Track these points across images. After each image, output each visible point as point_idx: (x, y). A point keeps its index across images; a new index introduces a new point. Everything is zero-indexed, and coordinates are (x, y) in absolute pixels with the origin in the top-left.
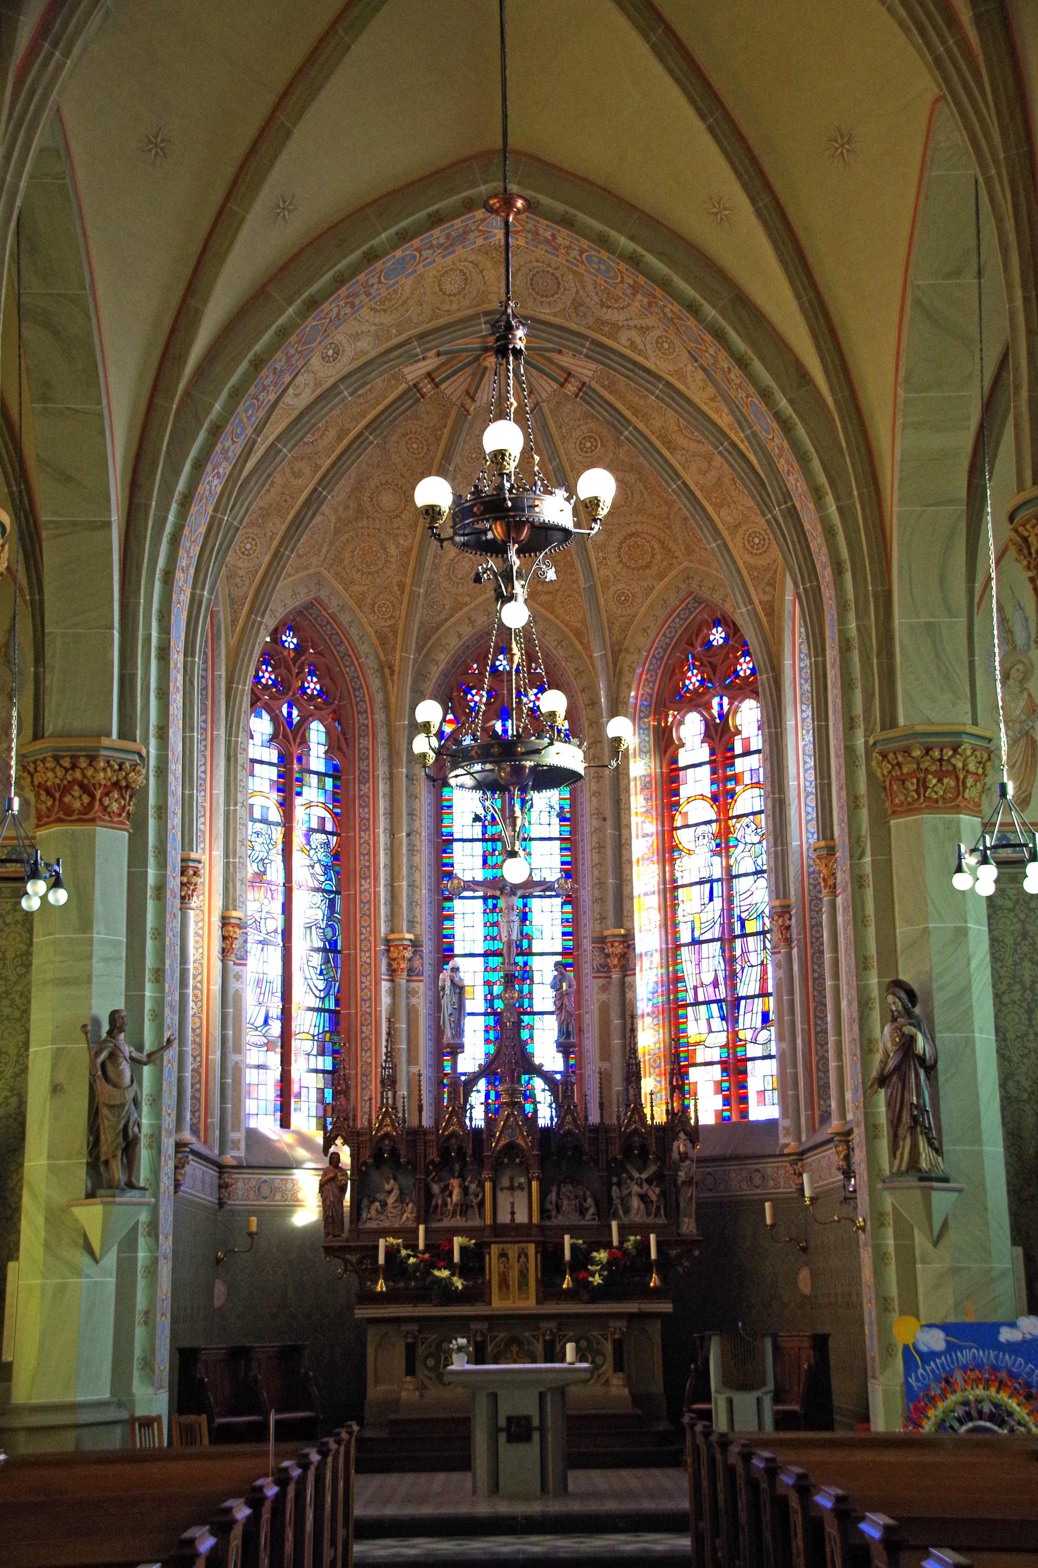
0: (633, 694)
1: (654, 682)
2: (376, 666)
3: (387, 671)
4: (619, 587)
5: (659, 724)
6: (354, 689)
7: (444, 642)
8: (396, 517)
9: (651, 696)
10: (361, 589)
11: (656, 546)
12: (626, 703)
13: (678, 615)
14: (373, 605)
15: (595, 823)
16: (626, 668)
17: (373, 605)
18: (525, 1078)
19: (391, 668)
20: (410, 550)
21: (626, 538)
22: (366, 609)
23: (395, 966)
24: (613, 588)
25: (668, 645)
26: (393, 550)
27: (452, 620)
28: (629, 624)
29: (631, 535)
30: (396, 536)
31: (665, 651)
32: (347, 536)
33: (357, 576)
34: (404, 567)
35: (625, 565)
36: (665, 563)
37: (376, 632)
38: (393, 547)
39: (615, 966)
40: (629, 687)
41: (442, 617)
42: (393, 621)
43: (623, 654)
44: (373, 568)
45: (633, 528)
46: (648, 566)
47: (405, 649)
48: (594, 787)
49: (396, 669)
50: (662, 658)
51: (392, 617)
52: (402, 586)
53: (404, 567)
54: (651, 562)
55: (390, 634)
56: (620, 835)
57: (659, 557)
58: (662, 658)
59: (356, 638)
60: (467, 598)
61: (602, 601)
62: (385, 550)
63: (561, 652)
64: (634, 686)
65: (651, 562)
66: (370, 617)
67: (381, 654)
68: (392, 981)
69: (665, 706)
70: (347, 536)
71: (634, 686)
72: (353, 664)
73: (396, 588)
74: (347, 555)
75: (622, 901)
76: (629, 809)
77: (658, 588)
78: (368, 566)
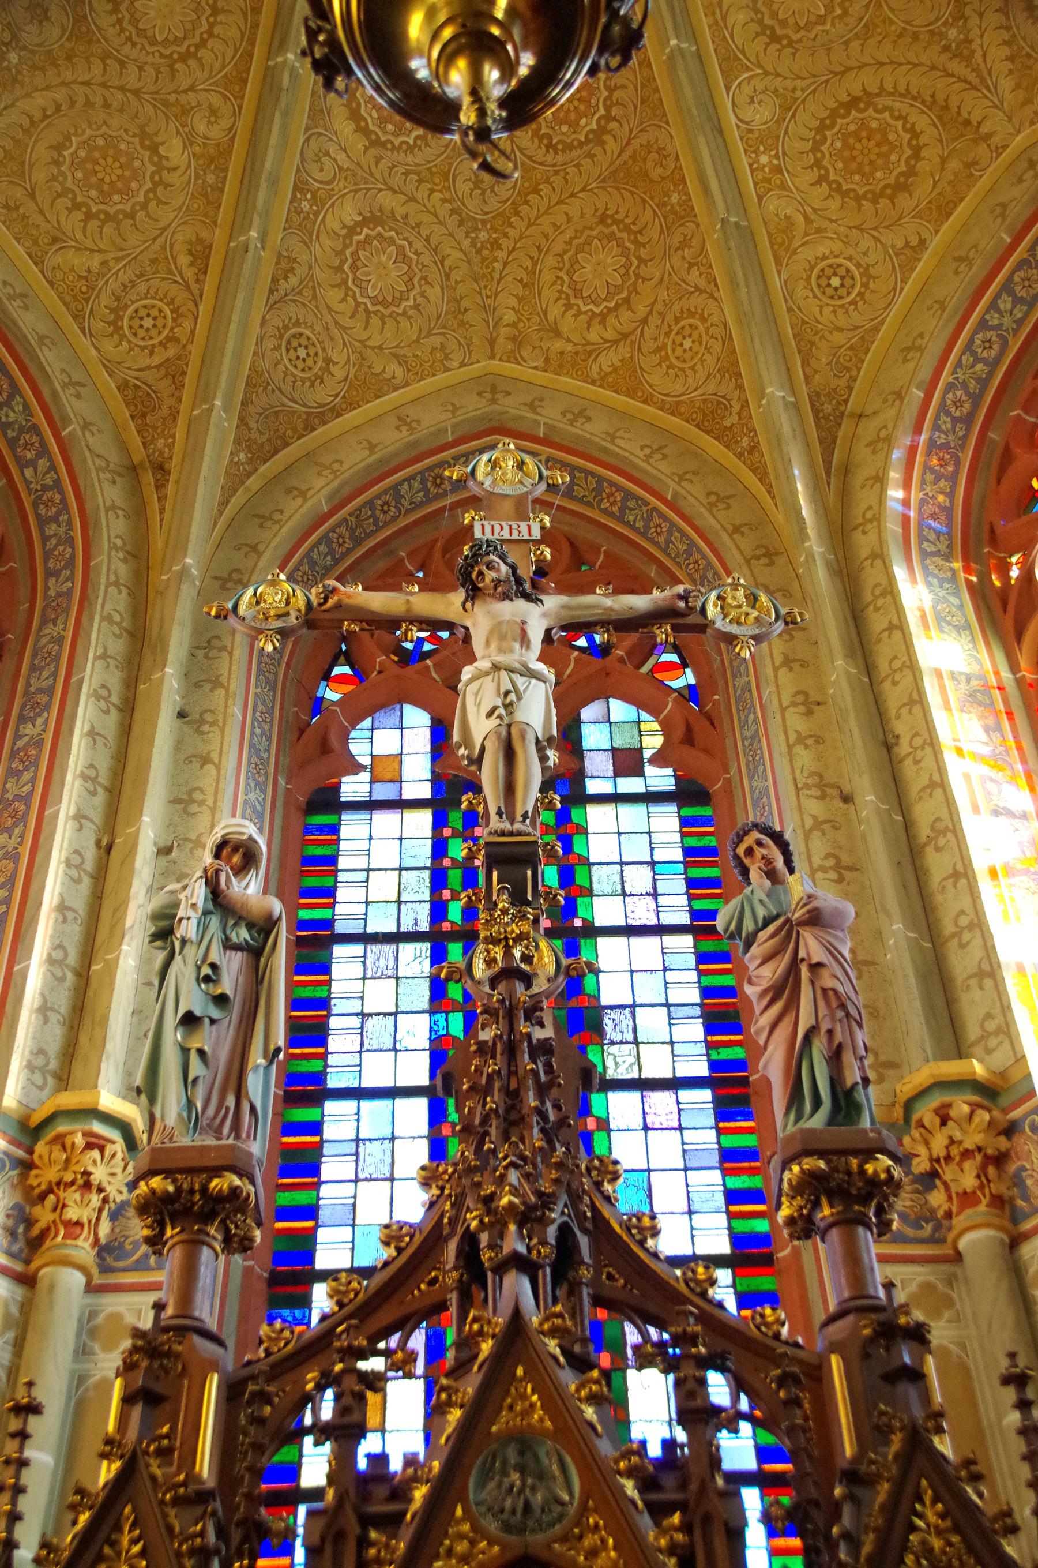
0: (895, 493)
1: (953, 478)
2: (114, 457)
3: (148, 478)
4: (821, 250)
5: (985, 578)
6: (42, 522)
7: (326, 459)
8: (184, 58)
9: (949, 512)
10: (79, 261)
11: (922, 123)
12: (878, 519)
13: (1007, 287)
14: (117, 312)
15: (814, 807)
16: (862, 452)
17: (117, 312)
18: (596, 1100)
19: (161, 469)
20: (225, 152)
21: (834, 115)
22: (98, 325)
23: (44, 1215)
24: (806, 254)
25: (984, 383)
26: (174, 151)
27: (352, 417)
28: (860, 348)
29: (852, 103)
30: (186, 111)
31: (976, 400)
32: (40, 100)
33: (72, 222)
34: (211, 197)
35: (837, 188)
36: (954, 165)
37: (123, 386)
38: (176, 142)
39: (967, 1199)
40: (880, 480)
41: (322, 395)
42: (172, 351)
43: (846, 425)
44: (118, 204)
45: (853, 84)
46: (902, 187)
47: (204, 394)
48: (796, 722)
49: (174, 466)
50: (968, 420)
51: (172, 339)
52: (201, 254)
53: (211, 197)
54: (911, 172)
55: (164, 387)
56: (908, 826)
57: (931, 154)
58: (968, 420)
59: (58, 379)
60: (395, 369)
61: (776, 282)
62: (154, 149)
63: (663, 466)
64: (895, 475)
65: (911, 172)
66: (109, 346)
67: (135, 439)
68: (27, 1280)
69: (993, 539)
70: (40, 100)
71: (895, 475)
72: (44, 451)
73: (184, 260)
74: (41, 151)
75: (950, 1002)
76: (932, 743)
77: (935, 243)
78: (105, 197)
